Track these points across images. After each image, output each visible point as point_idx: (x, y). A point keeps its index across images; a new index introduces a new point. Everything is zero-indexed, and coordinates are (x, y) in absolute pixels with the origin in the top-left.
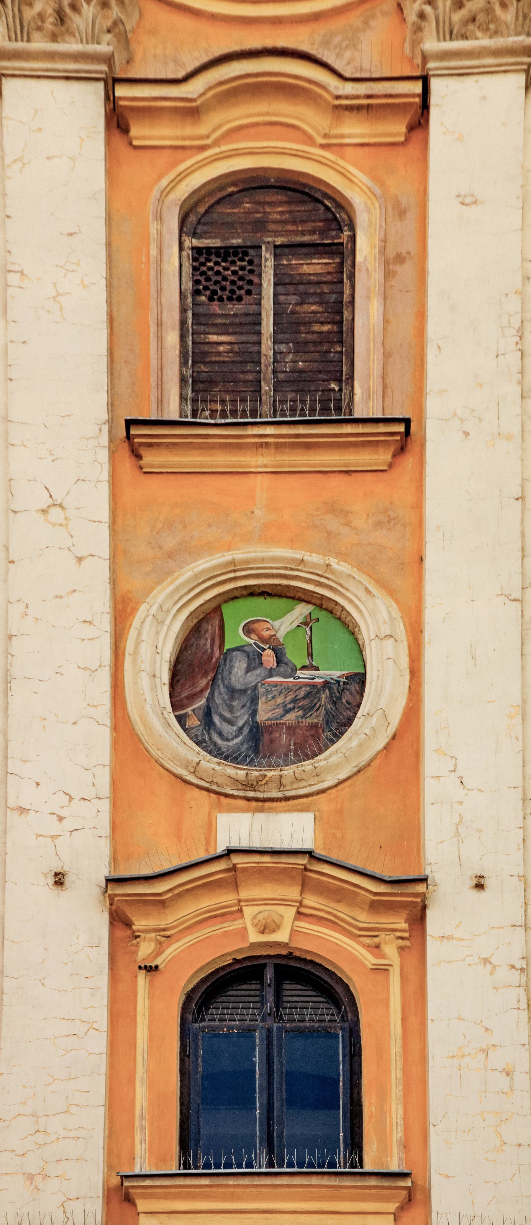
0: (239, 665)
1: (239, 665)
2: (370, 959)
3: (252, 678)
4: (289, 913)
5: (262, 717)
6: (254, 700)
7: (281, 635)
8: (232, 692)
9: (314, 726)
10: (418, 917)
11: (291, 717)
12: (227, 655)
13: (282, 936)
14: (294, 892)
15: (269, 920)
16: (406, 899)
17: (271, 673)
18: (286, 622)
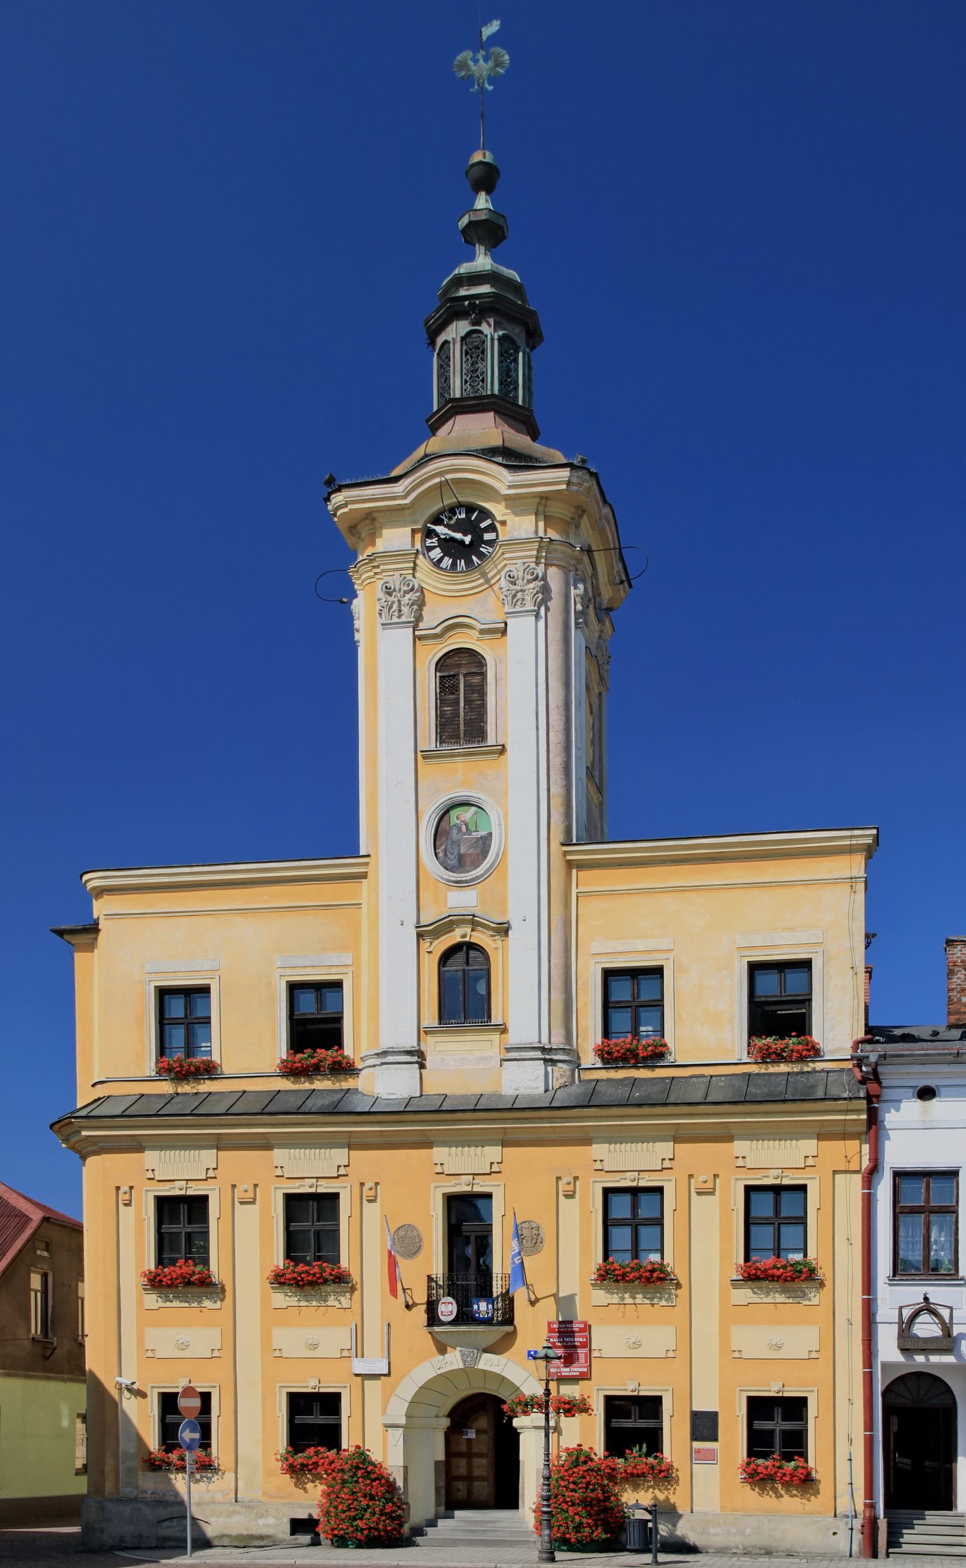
0: (455, 832)
1: (455, 832)
3: (459, 837)
4: (468, 930)
5: (462, 851)
6: (459, 846)
7: (467, 820)
8: (453, 842)
9: (477, 854)
11: (470, 851)
12: (451, 828)
13: (467, 939)
17: (464, 834)
18: (467, 814)
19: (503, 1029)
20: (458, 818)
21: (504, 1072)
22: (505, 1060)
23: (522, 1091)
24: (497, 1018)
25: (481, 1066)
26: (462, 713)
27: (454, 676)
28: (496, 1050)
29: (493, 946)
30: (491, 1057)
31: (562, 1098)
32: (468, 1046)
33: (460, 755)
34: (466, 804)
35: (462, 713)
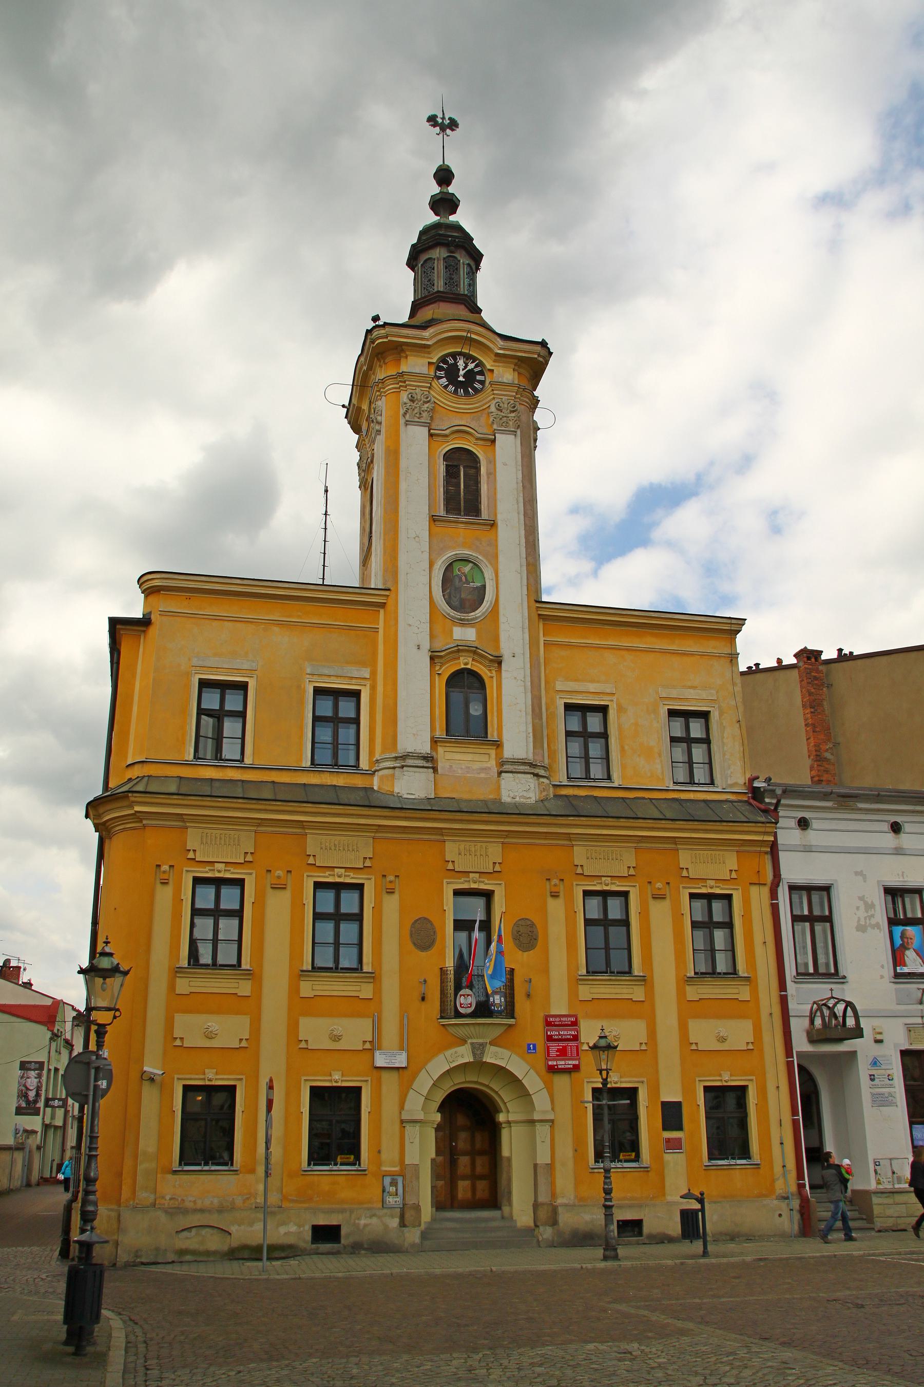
0: (457, 580)
1: (457, 580)
2: (490, 674)
10: (500, 663)
13: (469, 667)
14: (472, 655)
15: (465, 662)
16: (498, 662)
18: (467, 568)
19: (498, 745)
20: (459, 570)
21: (503, 782)
22: (501, 772)
23: (518, 799)
24: (493, 736)
25: (482, 775)
26: (462, 493)
27: (456, 466)
28: (493, 763)
29: (490, 674)
30: (490, 768)
31: (554, 807)
32: (469, 757)
33: (462, 523)
34: (466, 560)
35: (462, 493)
